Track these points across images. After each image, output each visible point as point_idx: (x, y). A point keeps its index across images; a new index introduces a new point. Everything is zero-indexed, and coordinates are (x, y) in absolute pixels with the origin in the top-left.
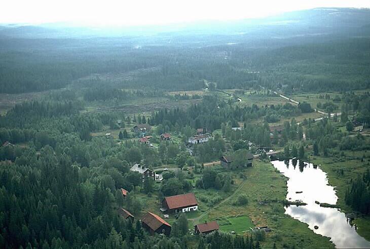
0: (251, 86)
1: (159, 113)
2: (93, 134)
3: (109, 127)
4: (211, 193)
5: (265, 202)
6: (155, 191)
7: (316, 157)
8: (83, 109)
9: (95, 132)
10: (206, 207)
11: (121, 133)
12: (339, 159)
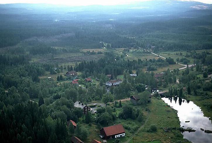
0: (132, 46)
1: (81, 63)
2: (40, 78)
3: (49, 72)
4: (130, 123)
5: (169, 129)
6: (92, 121)
7: (189, 95)
8: (30, 60)
9: (41, 76)
10: (130, 134)
11: (58, 76)
12: (205, 97)
